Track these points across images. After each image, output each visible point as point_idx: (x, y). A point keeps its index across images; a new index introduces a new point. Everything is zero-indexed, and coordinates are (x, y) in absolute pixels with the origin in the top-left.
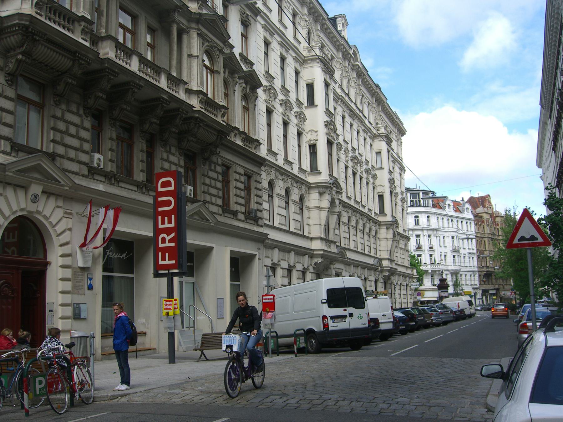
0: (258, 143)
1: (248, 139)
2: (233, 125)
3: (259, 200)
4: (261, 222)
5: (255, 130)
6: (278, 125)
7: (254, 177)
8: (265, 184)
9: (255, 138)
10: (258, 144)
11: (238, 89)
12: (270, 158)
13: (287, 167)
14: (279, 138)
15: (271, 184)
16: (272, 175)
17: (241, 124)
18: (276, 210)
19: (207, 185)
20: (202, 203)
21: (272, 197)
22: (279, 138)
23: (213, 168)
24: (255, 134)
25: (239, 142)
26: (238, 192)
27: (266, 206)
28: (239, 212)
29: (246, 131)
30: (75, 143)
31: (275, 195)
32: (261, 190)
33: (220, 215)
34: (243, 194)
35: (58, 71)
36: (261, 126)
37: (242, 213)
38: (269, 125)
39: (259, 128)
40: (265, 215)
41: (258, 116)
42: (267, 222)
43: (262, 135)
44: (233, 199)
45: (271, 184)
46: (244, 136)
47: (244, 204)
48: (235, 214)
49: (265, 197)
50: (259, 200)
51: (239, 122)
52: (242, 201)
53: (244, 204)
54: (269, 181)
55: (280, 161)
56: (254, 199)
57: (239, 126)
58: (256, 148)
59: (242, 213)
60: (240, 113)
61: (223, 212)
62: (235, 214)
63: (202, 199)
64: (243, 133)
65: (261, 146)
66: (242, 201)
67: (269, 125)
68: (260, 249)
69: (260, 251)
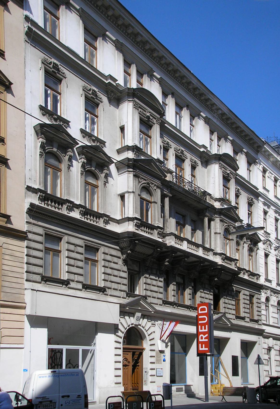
0: (258, 276)
1: (252, 274)
2: (242, 268)
3: (259, 309)
4: (260, 322)
5: (257, 268)
6: (273, 263)
7: (256, 296)
8: (263, 299)
9: (256, 273)
10: (258, 276)
11: (246, 246)
14: (273, 271)
15: (267, 299)
16: (268, 294)
17: (247, 266)
18: (271, 314)
19: (226, 303)
20: (223, 314)
21: (268, 307)
22: (273, 271)
23: (230, 293)
24: (257, 271)
25: (246, 277)
26: (246, 306)
27: (264, 312)
28: (246, 317)
29: (251, 270)
31: (270, 306)
32: (260, 303)
33: (234, 319)
34: (248, 307)
35: (147, 255)
36: (261, 265)
37: (248, 317)
38: (266, 263)
39: (259, 266)
40: (263, 318)
41: (259, 259)
42: (265, 322)
43: (261, 271)
44: (242, 310)
45: (267, 299)
46: (250, 273)
47: (249, 312)
49: (263, 307)
50: (259, 309)
51: (246, 265)
52: (248, 311)
53: (249, 312)
54: (266, 297)
56: (256, 309)
57: (246, 267)
58: (257, 279)
59: (248, 317)
60: (247, 260)
61: (236, 318)
62: (243, 318)
63: (223, 312)
64: (249, 271)
65: (260, 277)
66: (248, 311)
67: (266, 263)
68: (260, 338)
69: (260, 340)
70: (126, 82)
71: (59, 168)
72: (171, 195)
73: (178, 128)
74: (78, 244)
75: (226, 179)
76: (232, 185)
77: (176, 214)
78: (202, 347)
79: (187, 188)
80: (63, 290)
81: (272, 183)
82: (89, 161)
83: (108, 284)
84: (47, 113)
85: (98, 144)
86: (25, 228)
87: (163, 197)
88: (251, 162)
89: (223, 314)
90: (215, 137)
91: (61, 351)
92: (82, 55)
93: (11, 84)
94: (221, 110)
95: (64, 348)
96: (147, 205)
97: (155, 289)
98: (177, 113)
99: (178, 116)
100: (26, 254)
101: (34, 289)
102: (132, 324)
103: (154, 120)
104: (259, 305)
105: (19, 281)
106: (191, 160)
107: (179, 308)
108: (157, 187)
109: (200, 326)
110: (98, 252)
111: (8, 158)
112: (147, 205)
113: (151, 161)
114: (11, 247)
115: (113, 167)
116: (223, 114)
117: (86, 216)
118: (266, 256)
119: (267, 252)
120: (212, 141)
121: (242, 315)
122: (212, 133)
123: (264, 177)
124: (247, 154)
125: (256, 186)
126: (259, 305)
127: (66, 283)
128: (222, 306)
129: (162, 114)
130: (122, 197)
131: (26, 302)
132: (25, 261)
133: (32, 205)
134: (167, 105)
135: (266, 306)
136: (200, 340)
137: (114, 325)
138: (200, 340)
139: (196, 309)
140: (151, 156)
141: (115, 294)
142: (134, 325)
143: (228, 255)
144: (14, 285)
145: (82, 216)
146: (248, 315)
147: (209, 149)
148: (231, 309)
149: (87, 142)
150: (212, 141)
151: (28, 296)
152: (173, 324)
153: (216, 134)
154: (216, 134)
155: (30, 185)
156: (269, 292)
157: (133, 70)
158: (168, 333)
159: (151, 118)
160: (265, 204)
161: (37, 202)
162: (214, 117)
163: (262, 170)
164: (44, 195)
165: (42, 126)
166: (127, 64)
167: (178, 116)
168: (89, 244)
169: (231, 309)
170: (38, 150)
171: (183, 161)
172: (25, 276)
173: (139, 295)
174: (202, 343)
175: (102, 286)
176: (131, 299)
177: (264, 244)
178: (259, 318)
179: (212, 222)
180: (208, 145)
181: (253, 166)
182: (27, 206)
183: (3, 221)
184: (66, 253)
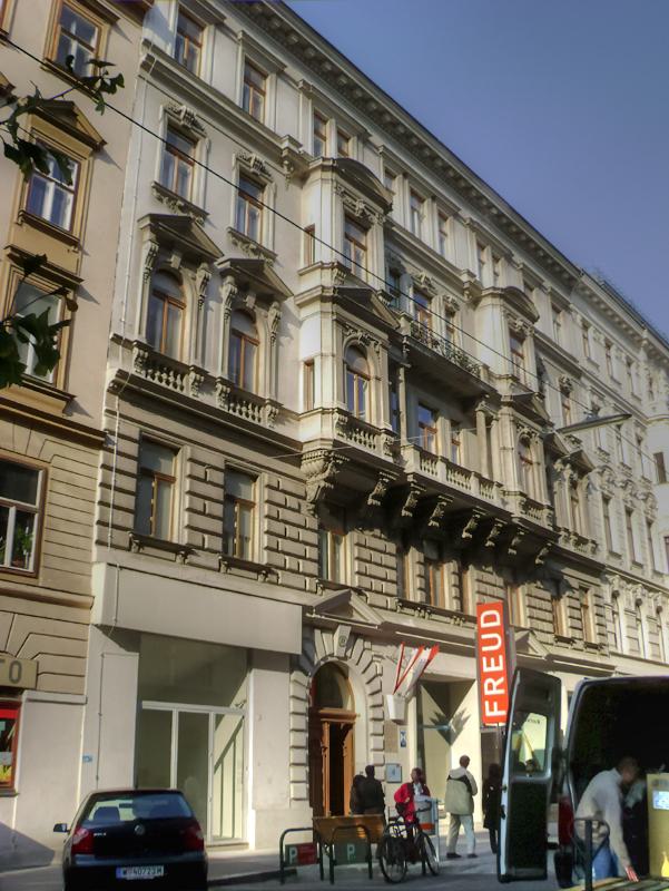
1: (581, 541)
4: (606, 651)
12: (613, 563)
13: (636, 572)
30: (380, 572)
42: (613, 649)
48: (570, 641)
55: (627, 566)
59: (580, 640)
62: (570, 641)
70: (317, 147)
71: (180, 303)
72: (409, 366)
73: (417, 236)
74: (213, 464)
75: (517, 337)
76: (528, 349)
77: (420, 407)
78: (491, 709)
79: (439, 350)
80: (177, 568)
81: (603, 351)
82: (243, 287)
83: (278, 559)
84: (165, 195)
85: (262, 257)
86: (103, 423)
87: (393, 367)
88: (559, 307)
89: (526, 632)
90: (486, 256)
91: (170, 714)
92: (238, 101)
93: (104, 143)
94: (496, 208)
95: (176, 709)
96: (360, 383)
97: (380, 572)
98: (413, 209)
99: (416, 214)
100: (99, 481)
101: (115, 563)
102: (332, 655)
103: (372, 216)
104: (601, 611)
105: (81, 542)
106: (445, 299)
107: (434, 616)
108: (384, 347)
109: (484, 659)
110: (255, 481)
111: (81, 277)
112: (360, 383)
113: (365, 294)
114: (69, 465)
115: (290, 303)
116: (500, 215)
117: (232, 405)
118: (606, 500)
119: (606, 492)
120: (483, 263)
121: (566, 633)
122: (481, 247)
123: (585, 338)
124: (553, 294)
125: (574, 356)
126: (601, 611)
127: (185, 551)
128: (525, 613)
129: (388, 208)
130: (310, 364)
131: (93, 593)
132: (98, 498)
133: (121, 374)
134: (394, 194)
135: (614, 613)
136: (487, 692)
137: (288, 658)
138: (487, 692)
139: (475, 620)
140: (366, 284)
141: (290, 583)
142: (334, 659)
143: (532, 497)
144: (71, 553)
145: (225, 402)
146: (578, 634)
147: (477, 278)
148: (544, 620)
149: (239, 254)
150: (483, 263)
151: (98, 579)
152: (426, 654)
153: (488, 250)
154: (488, 250)
155: (120, 333)
156: (616, 581)
157: (329, 130)
158: (409, 679)
159: (368, 213)
160: (593, 392)
161: (132, 370)
162: (483, 220)
163: (580, 324)
164: (146, 354)
165: (154, 218)
166: (319, 119)
167: (416, 214)
168: (234, 463)
169: (544, 620)
170: (143, 267)
171: (429, 299)
172: (95, 532)
173: (346, 587)
174: (492, 699)
175: (264, 562)
176: (329, 594)
177: (601, 474)
178: (604, 640)
179: (494, 423)
180: (477, 273)
181: (564, 316)
182: (110, 375)
183: (59, 407)
184: (187, 484)
